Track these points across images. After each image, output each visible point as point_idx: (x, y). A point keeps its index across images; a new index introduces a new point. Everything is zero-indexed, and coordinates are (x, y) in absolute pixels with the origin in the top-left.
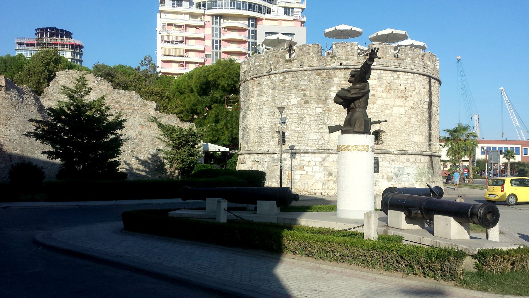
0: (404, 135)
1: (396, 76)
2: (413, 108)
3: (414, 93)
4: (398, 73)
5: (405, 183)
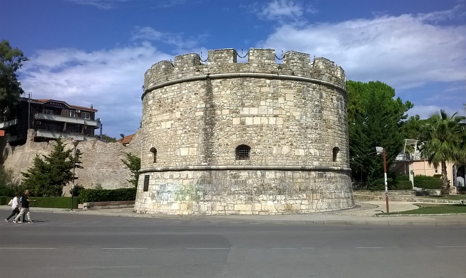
0: (169, 150)
1: (163, 91)
2: (179, 119)
3: (181, 103)
4: (165, 87)
5: (163, 200)
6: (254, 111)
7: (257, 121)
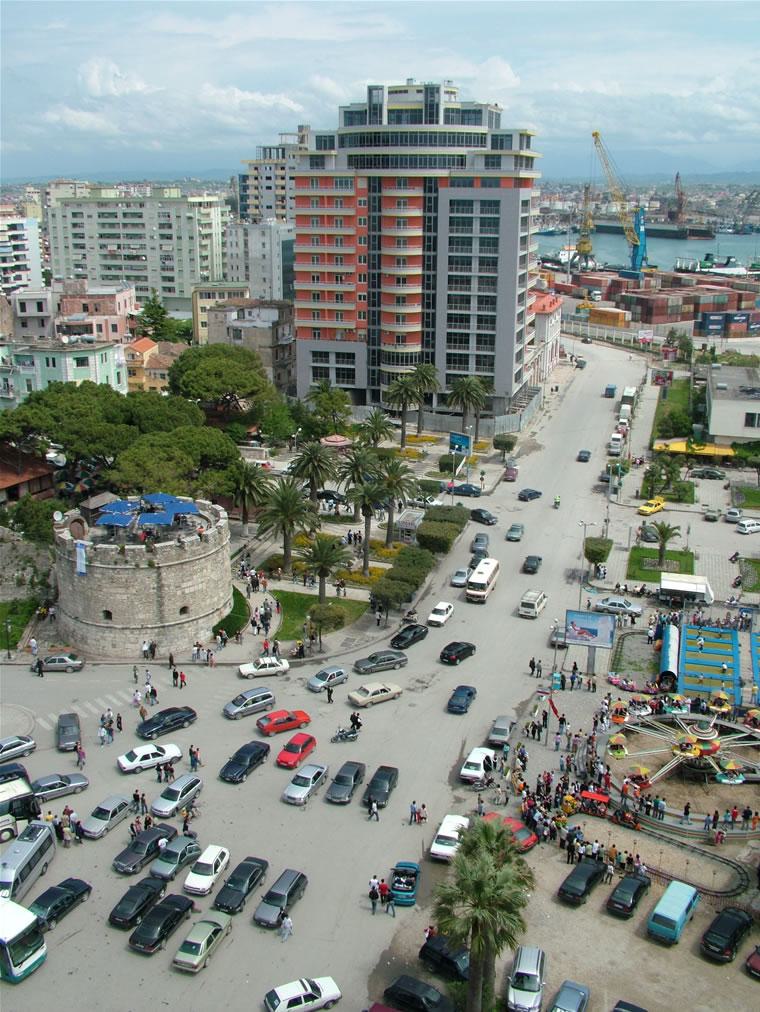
6: (190, 583)
7: (192, 589)
